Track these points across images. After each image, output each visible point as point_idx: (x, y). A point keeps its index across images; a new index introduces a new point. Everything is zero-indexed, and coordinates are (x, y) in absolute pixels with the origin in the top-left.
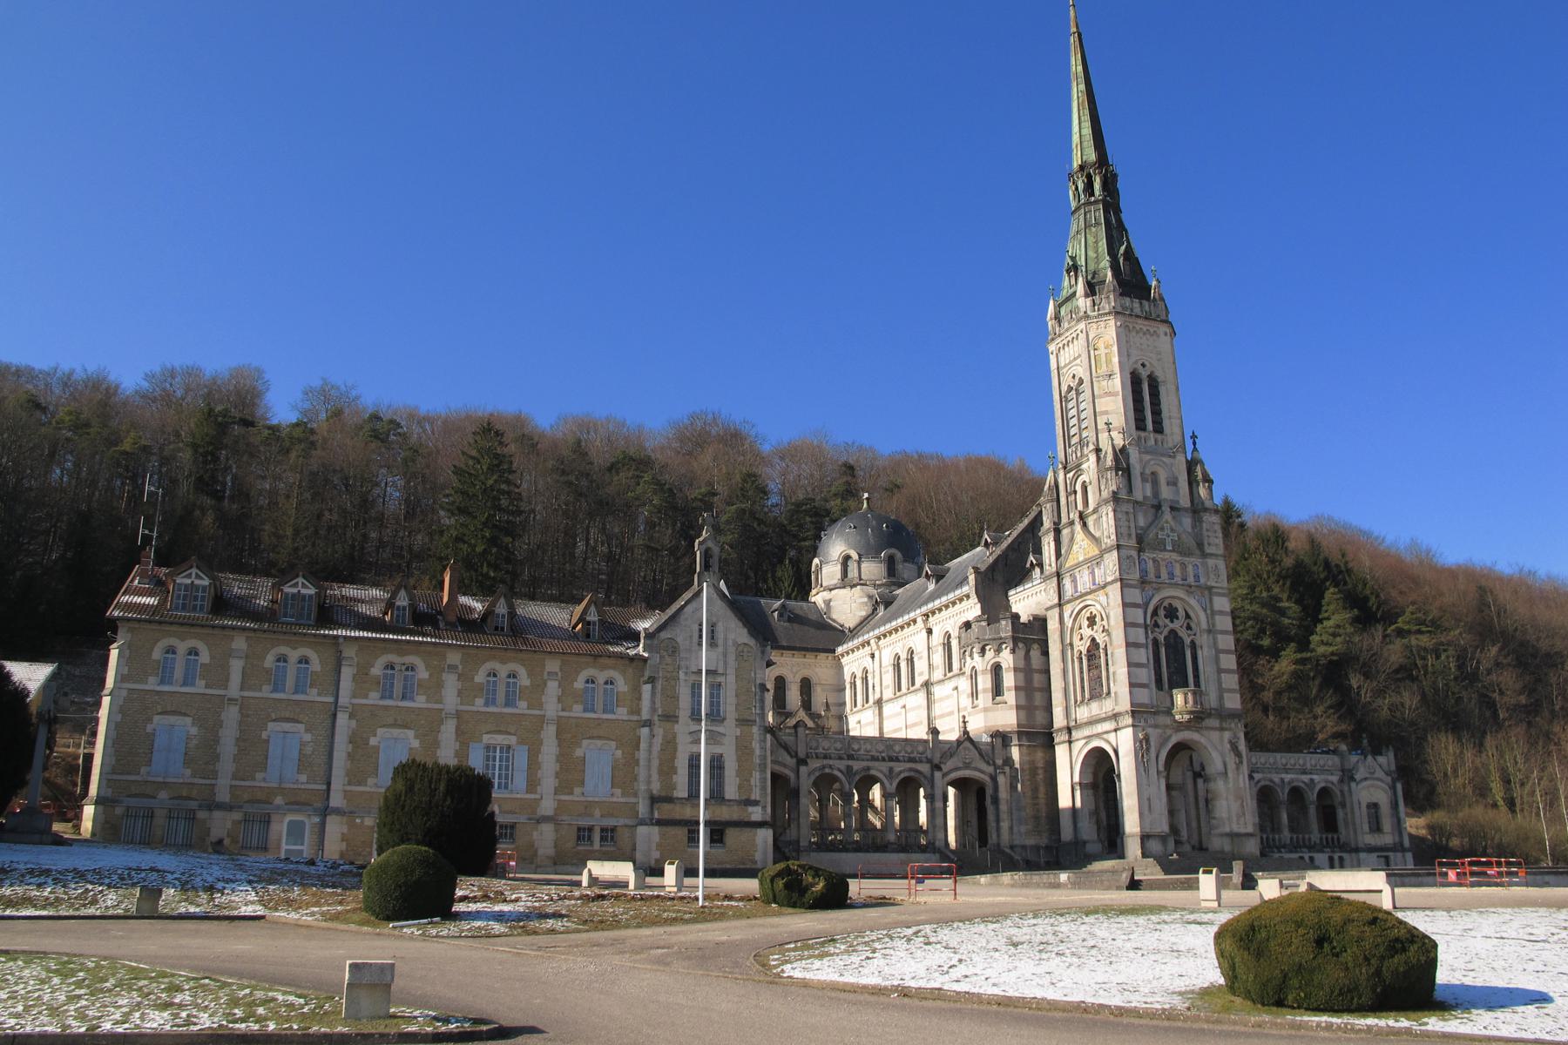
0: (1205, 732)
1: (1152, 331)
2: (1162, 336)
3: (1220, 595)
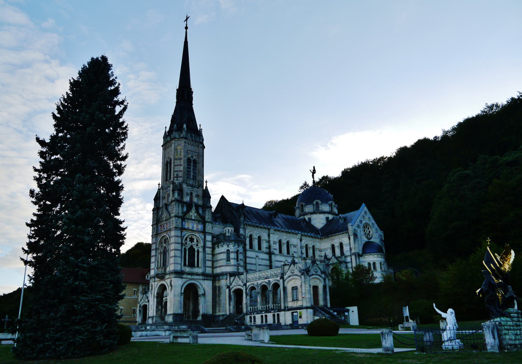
3: (173, 230)
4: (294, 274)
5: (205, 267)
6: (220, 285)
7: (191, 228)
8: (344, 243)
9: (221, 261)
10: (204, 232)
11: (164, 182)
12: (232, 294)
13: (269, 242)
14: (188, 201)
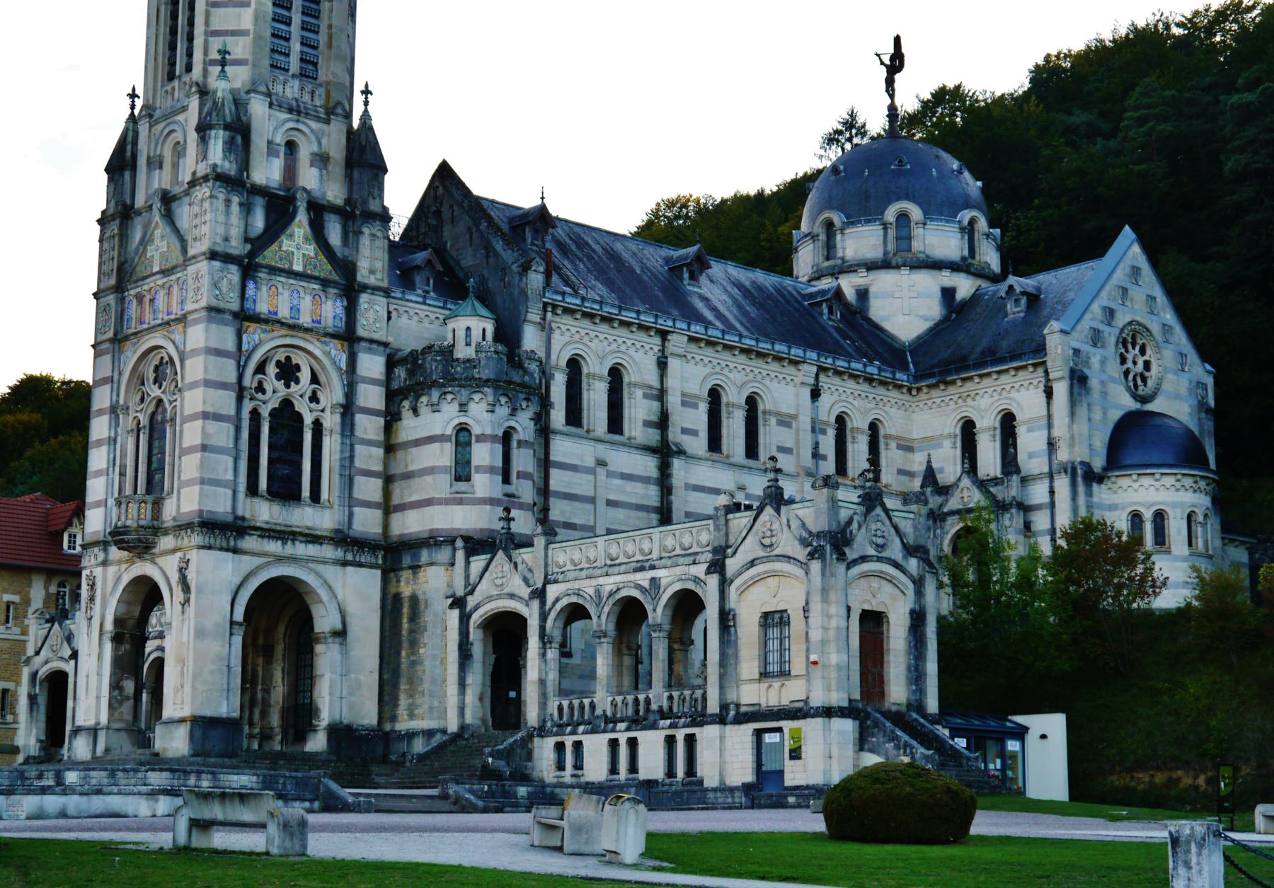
3: (196, 322)
4: (776, 552)
5: (351, 502)
6: (419, 593)
7: (284, 313)
8: (1019, 417)
9: (429, 479)
10: (349, 336)
11: (159, 84)
13: (661, 395)
14: (275, 185)
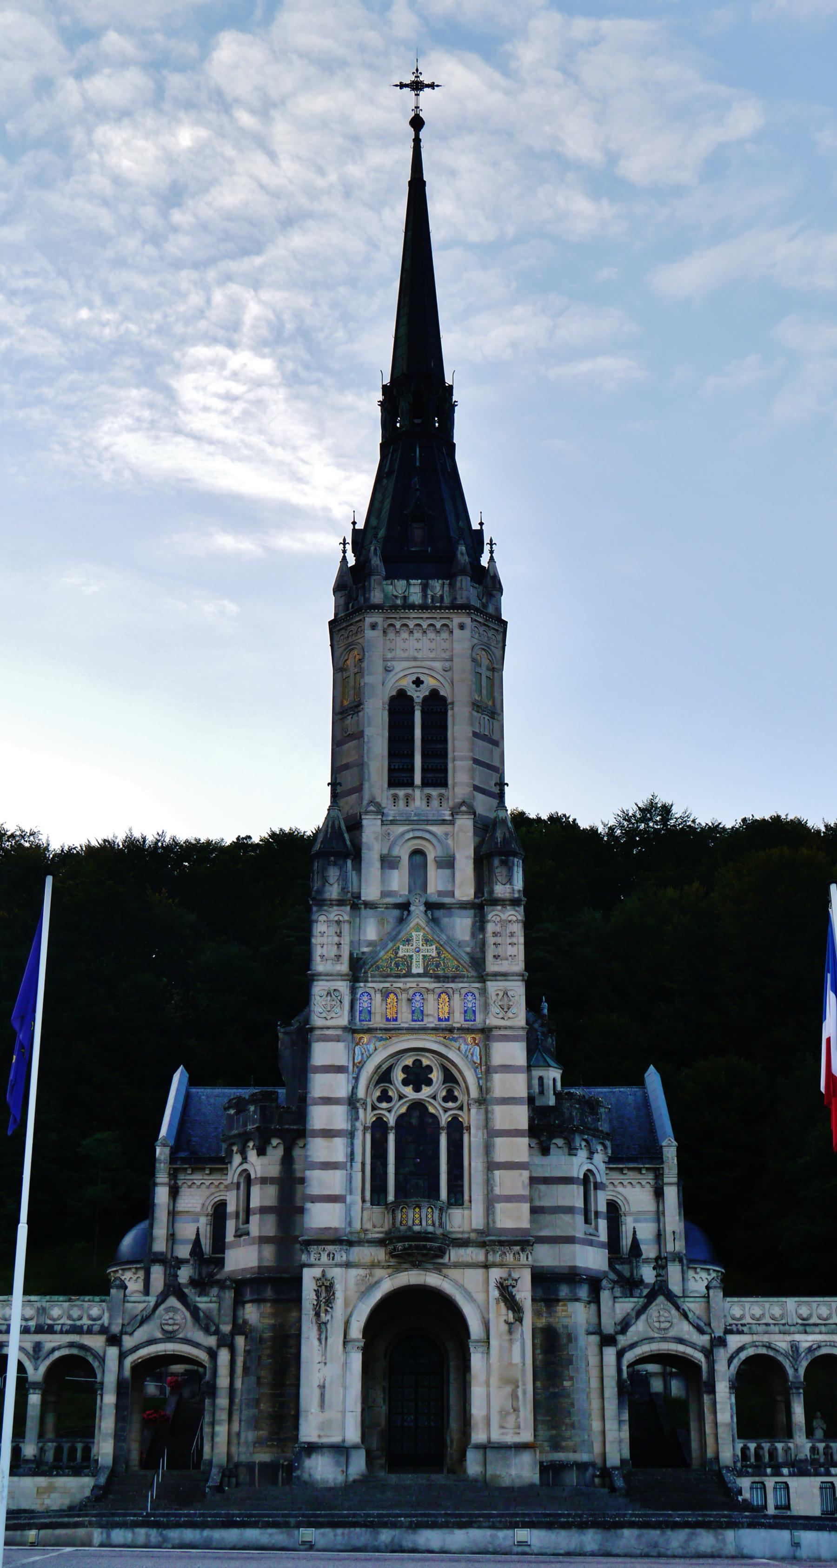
0: (453, 1273)
1: (438, 625)
2: (457, 631)
12: (624, 1368)
